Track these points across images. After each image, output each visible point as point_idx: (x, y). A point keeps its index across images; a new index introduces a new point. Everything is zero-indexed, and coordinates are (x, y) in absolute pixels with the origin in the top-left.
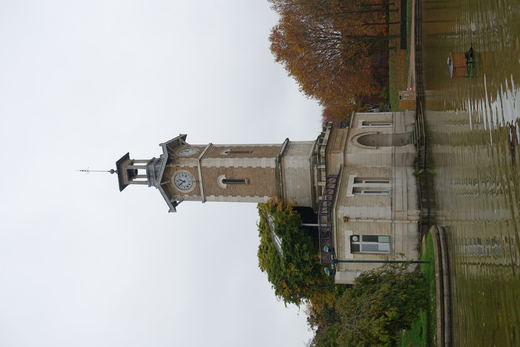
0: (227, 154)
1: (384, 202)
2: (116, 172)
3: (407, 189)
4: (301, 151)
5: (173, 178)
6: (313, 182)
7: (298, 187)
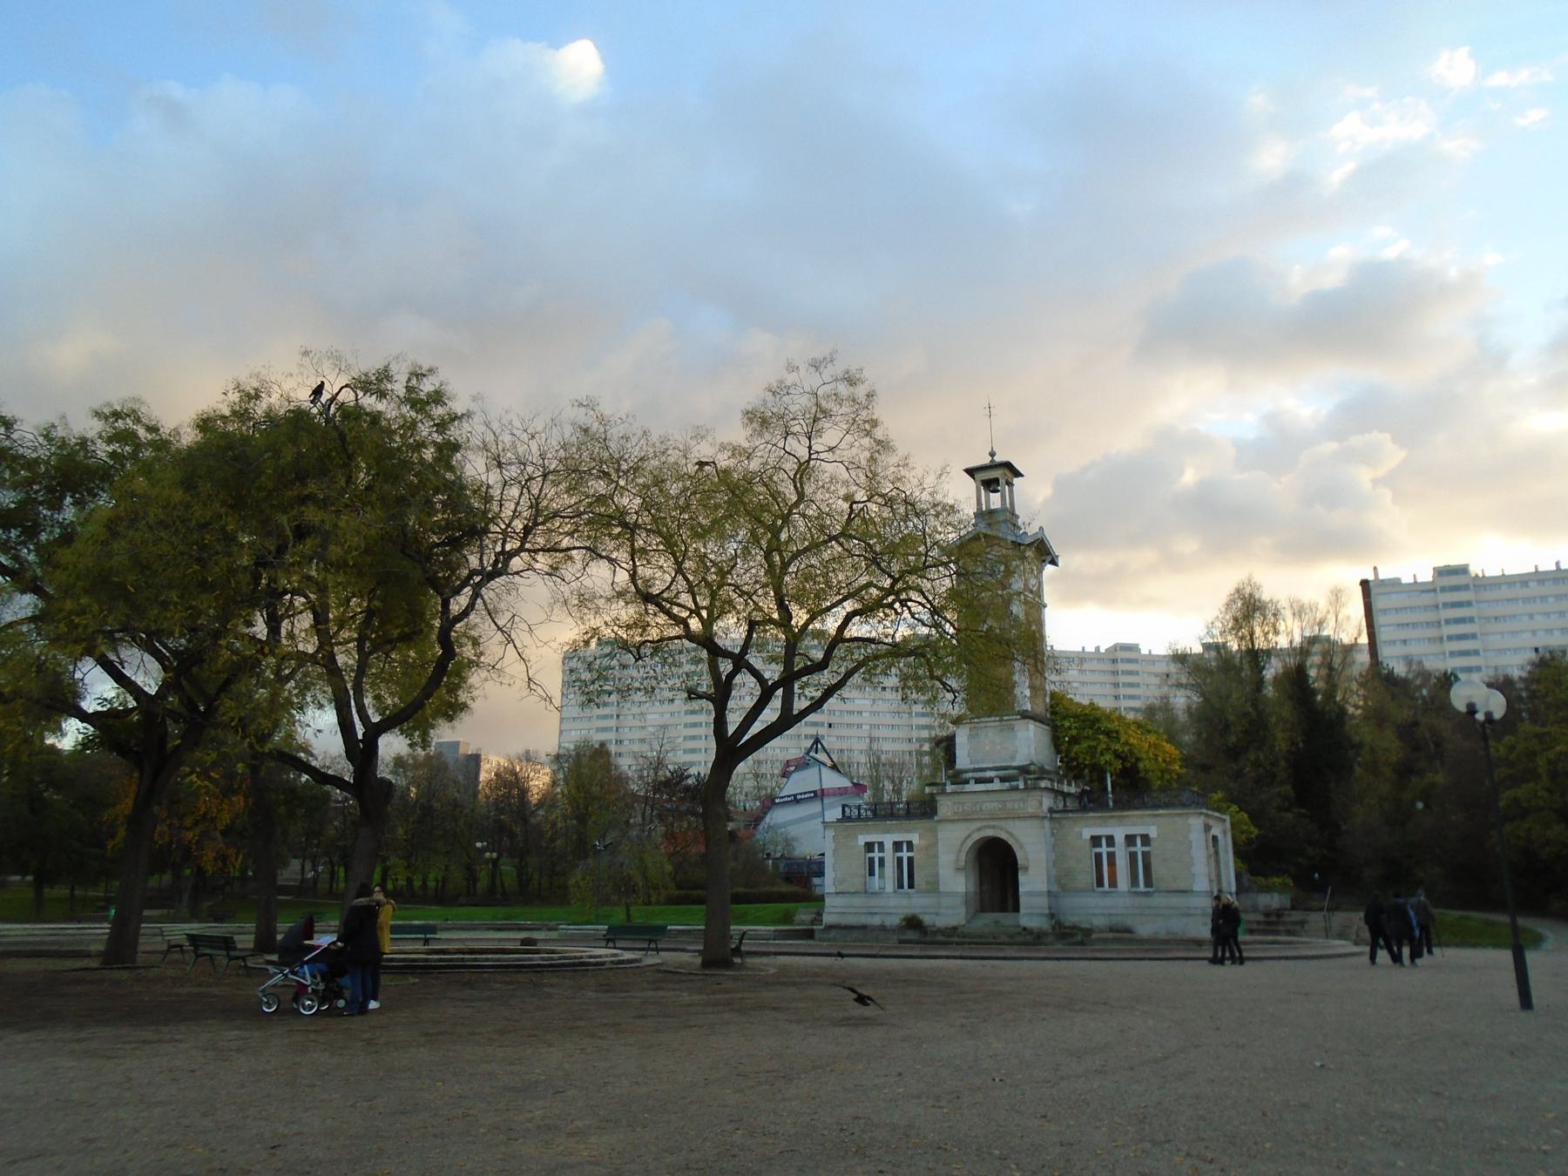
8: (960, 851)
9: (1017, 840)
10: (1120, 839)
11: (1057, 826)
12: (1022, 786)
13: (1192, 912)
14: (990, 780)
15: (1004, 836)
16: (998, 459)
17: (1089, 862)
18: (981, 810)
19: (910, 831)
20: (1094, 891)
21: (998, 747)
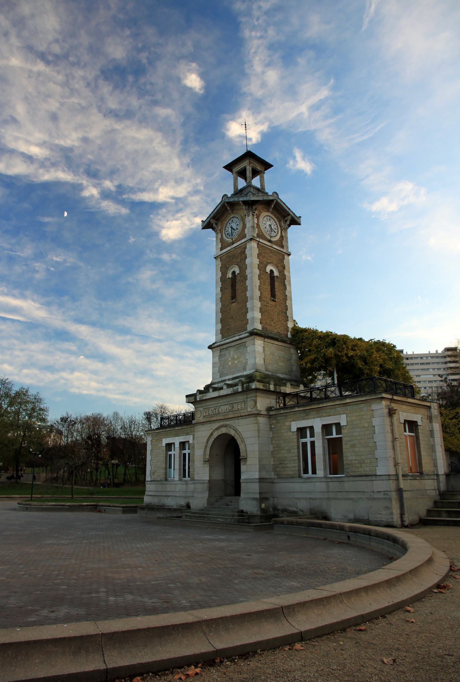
0: (230, 275)
1: (156, 474)
3: (169, 496)
4: (230, 363)
8: (206, 446)
10: (318, 430)
11: (274, 422)
13: (376, 496)
14: (221, 388)
15: (232, 433)
17: (296, 451)
18: (219, 413)
20: (300, 477)
21: (236, 362)
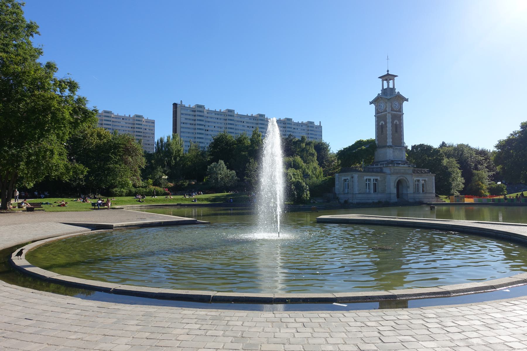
0: (395, 123)
2: (388, 73)
5: (382, 101)
6: (382, 162)
7: (381, 156)
9: (408, 180)
12: (411, 166)
13: (433, 197)
15: (405, 179)
16: (390, 73)
19: (377, 176)
